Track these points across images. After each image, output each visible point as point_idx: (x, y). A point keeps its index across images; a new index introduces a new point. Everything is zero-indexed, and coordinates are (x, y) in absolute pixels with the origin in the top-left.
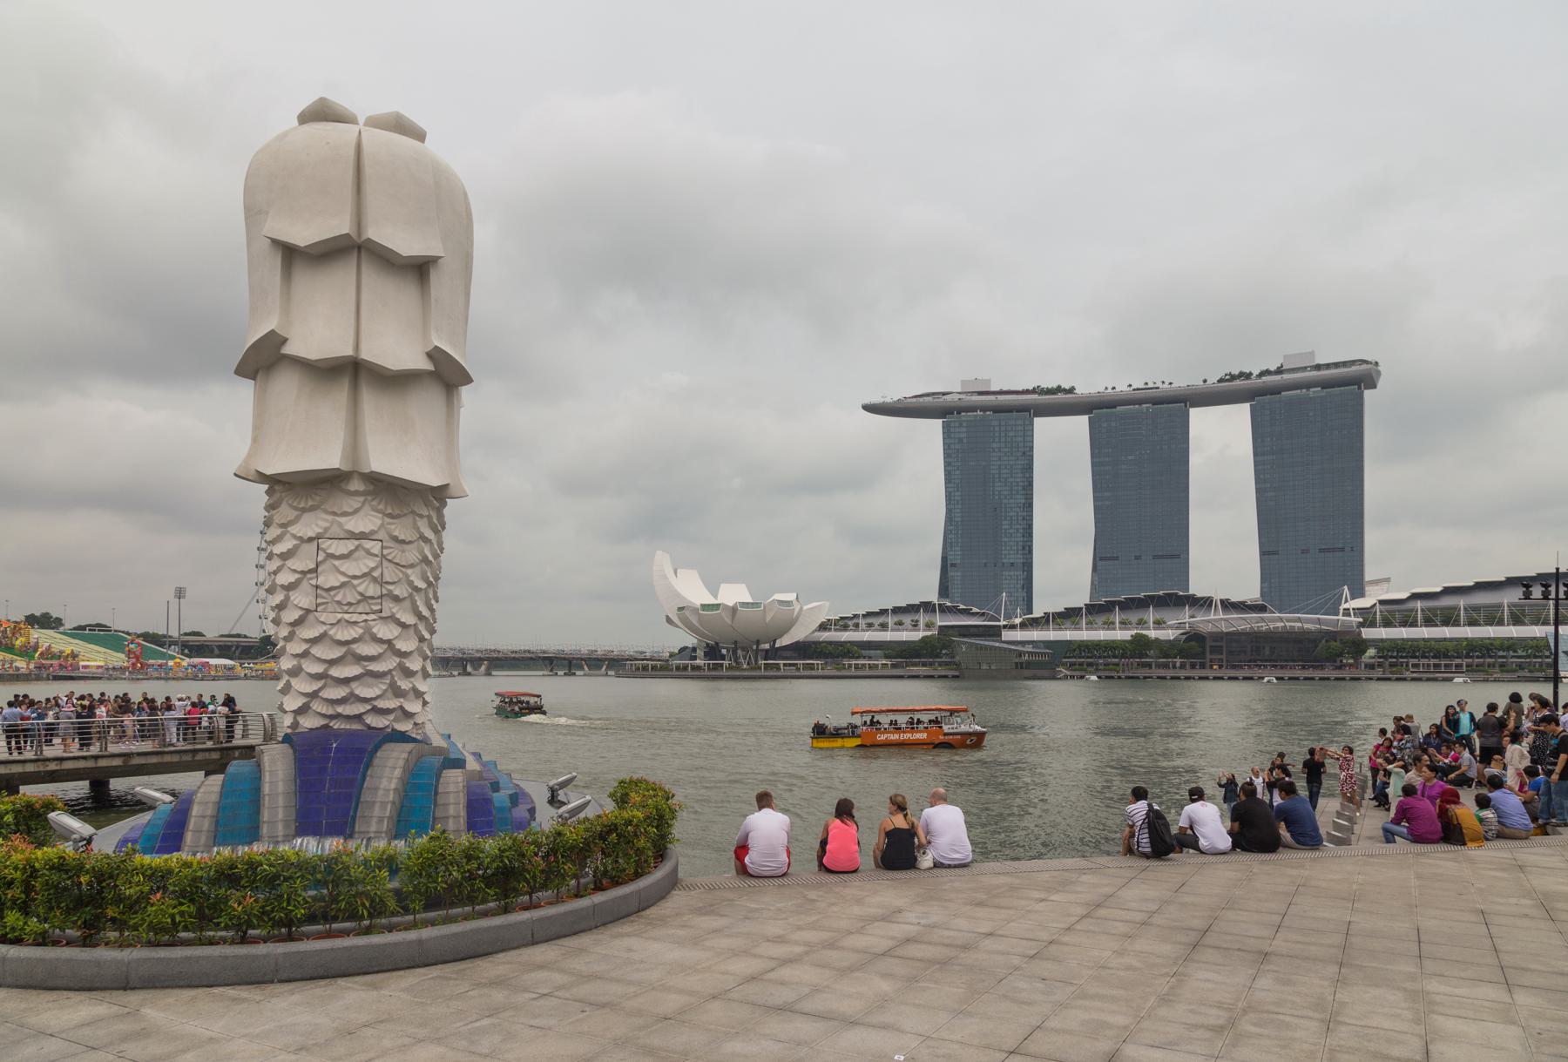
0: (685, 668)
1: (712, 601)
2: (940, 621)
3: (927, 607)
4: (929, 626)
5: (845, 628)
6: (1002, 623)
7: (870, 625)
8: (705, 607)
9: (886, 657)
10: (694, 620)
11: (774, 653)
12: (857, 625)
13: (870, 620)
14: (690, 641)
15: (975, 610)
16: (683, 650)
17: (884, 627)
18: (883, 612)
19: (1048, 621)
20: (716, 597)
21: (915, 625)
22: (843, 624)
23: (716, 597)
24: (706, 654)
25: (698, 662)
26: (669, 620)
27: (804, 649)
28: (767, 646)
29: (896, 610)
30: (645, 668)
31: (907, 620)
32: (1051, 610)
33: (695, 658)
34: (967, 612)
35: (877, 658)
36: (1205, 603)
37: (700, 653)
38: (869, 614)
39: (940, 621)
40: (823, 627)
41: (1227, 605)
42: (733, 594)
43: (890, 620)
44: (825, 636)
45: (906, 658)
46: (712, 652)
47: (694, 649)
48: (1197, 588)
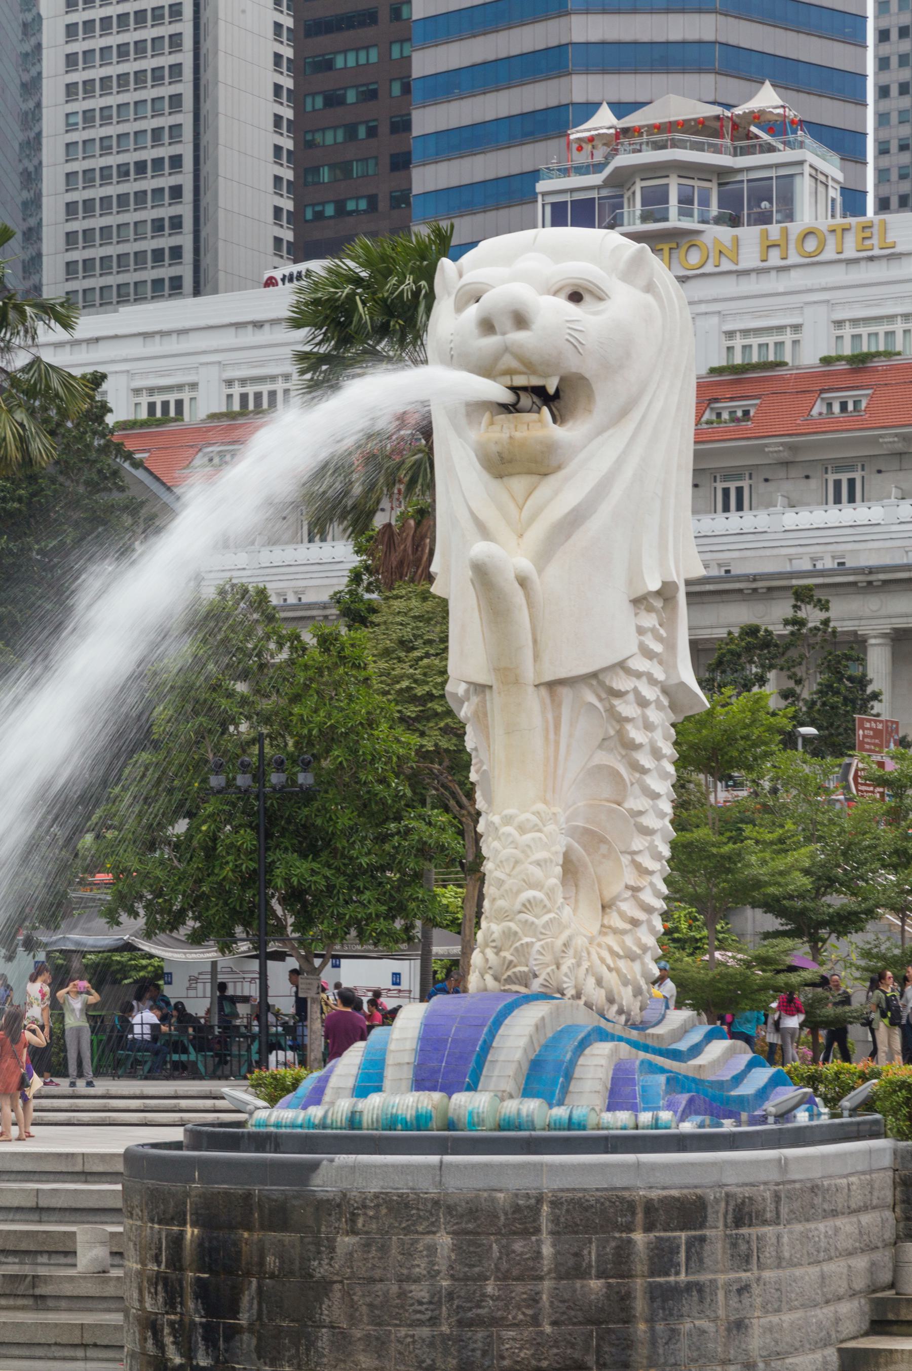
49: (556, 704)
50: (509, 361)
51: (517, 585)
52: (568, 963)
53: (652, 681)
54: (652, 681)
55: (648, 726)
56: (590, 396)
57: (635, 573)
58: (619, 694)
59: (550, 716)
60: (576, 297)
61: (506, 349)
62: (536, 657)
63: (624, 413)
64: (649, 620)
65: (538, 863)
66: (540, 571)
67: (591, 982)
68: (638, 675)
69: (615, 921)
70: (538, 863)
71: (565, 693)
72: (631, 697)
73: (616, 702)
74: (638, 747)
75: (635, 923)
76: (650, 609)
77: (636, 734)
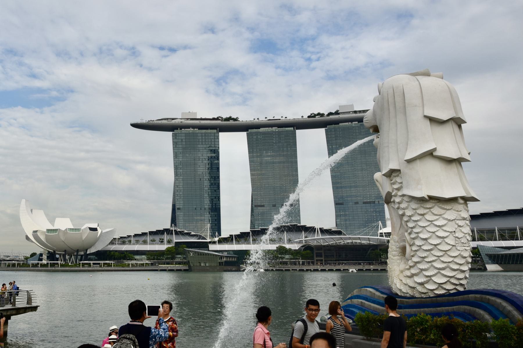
0: (36, 265)
1: (51, 227)
2: (176, 239)
3: (168, 231)
4: (169, 242)
5: (124, 243)
6: (208, 240)
7: (137, 242)
8: (48, 231)
9: (148, 259)
10: (43, 238)
11: (86, 257)
12: (130, 241)
13: (137, 238)
14: (39, 249)
15: (193, 233)
16: (33, 255)
17: (145, 242)
18: (144, 234)
19: (232, 239)
20: (53, 226)
21: (162, 242)
22: (123, 240)
23: (53, 226)
24: (48, 258)
25: (44, 262)
26: (27, 238)
27: (103, 255)
28: (82, 253)
29: (151, 233)
30: (14, 265)
31: (157, 238)
32: (234, 233)
33: (41, 260)
34: (189, 234)
35: (141, 260)
36: (311, 230)
37: (45, 257)
38: (136, 235)
39: (176, 239)
40: (112, 243)
41: (323, 231)
42: (63, 224)
43: (148, 238)
44: (113, 248)
45: (157, 260)
46: (51, 256)
47: (41, 255)
48: (305, 221)
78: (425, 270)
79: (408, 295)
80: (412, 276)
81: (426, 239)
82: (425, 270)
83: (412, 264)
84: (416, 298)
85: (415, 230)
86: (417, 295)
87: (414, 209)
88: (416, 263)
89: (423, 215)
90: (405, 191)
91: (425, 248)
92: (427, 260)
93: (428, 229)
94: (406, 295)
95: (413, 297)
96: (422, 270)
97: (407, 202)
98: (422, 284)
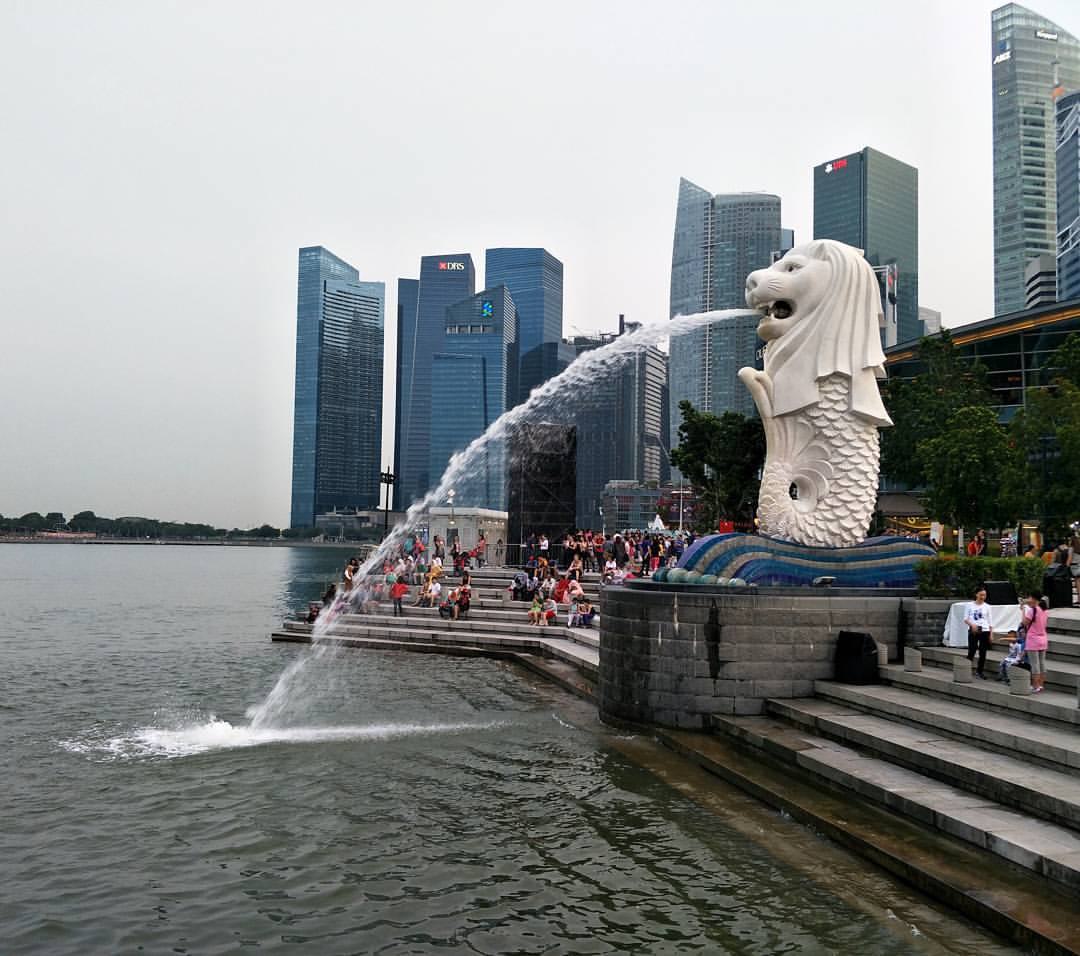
49: (784, 424)
50: (756, 300)
51: (755, 382)
52: (783, 521)
53: (838, 412)
54: (838, 412)
55: (837, 429)
56: (796, 305)
57: (816, 372)
58: (817, 418)
59: (782, 430)
60: (791, 270)
61: (753, 296)
62: (772, 407)
63: (811, 310)
64: (828, 388)
65: (770, 484)
66: (772, 377)
67: (795, 529)
68: (826, 410)
69: (822, 506)
70: (770, 484)
71: (788, 420)
72: (823, 418)
73: (815, 421)
74: (830, 437)
75: (832, 507)
76: (833, 383)
77: (829, 433)
78: (856, 512)
79: (823, 545)
80: (839, 518)
81: (866, 473)
82: (856, 512)
83: (839, 504)
84: (835, 548)
85: (851, 460)
86: (838, 545)
87: (859, 433)
88: (845, 502)
89: (866, 441)
90: (856, 407)
91: (862, 483)
92: (861, 499)
93: (870, 459)
94: (818, 545)
95: (828, 548)
96: (853, 511)
97: (846, 421)
98: (848, 530)
